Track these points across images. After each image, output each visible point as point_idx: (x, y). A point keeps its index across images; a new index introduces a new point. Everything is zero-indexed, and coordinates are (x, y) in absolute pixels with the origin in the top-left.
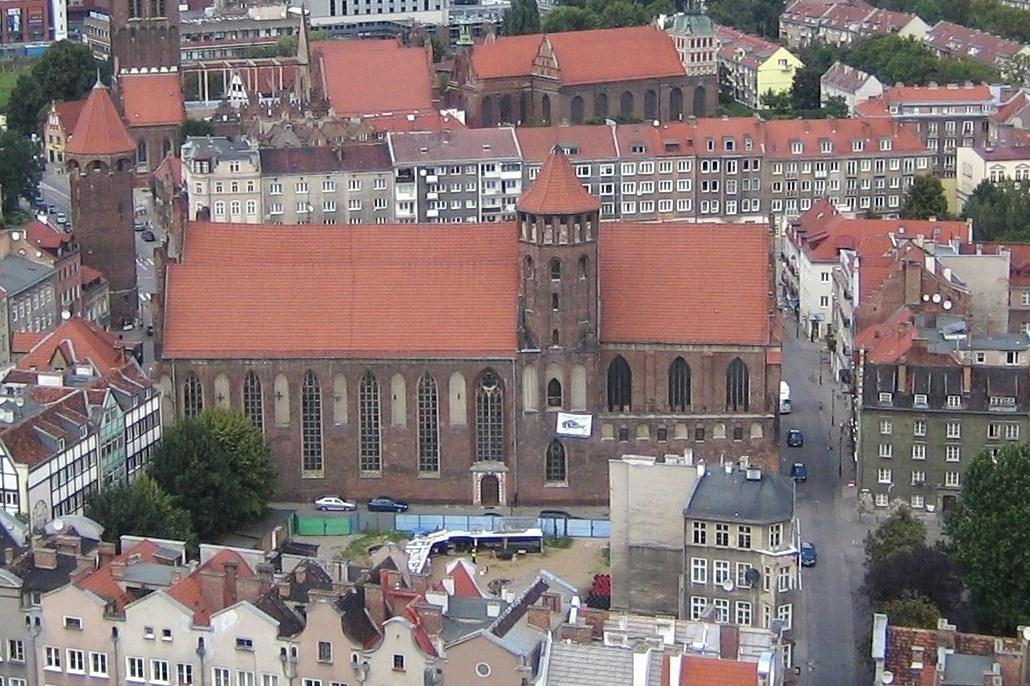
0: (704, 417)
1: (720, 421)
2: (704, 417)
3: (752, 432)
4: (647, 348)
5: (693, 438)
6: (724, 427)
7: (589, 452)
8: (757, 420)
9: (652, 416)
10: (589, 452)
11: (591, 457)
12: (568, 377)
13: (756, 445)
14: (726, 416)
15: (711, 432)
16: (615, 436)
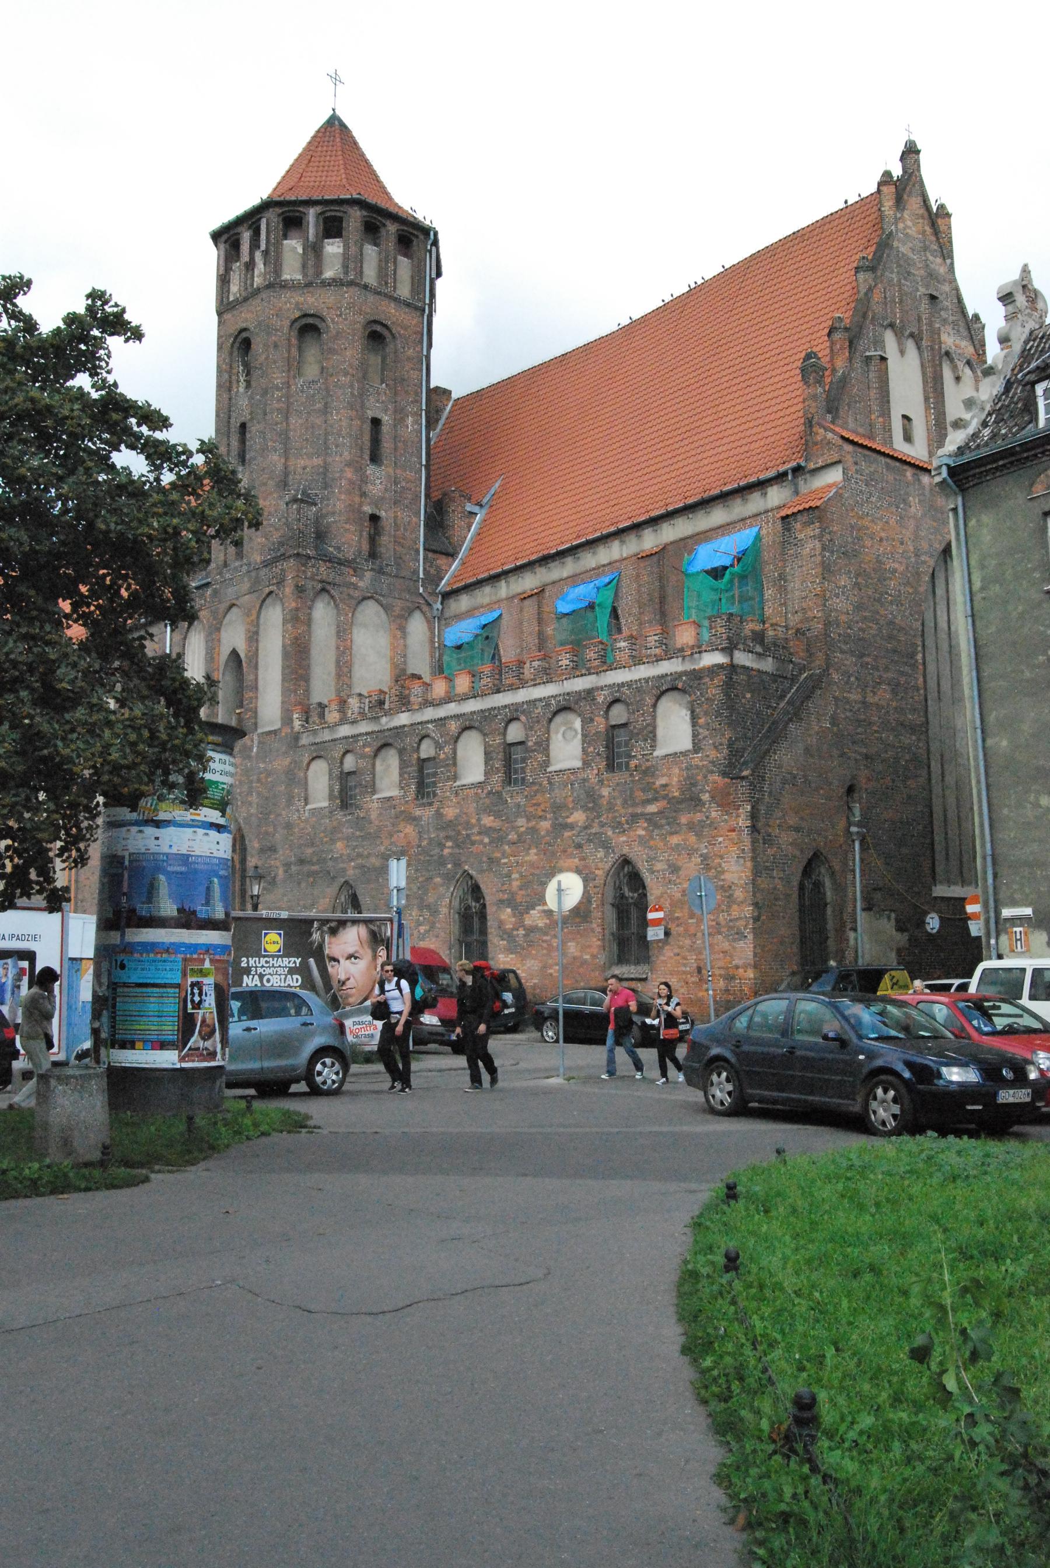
0: (522, 696)
1: (565, 707)
2: (522, 696)
3: (660, 732)
4: (528, 582)
5: (497, 778)
6: (578, 724)
7: (284, 854)
8: (668, 687)
9: (403, 719)
10: (284, 854)
11: (287, 865)
12: (253, 637)
13: (671, 779)
14: (580, 684)
15: (544, 746)
16: (331, 797)
